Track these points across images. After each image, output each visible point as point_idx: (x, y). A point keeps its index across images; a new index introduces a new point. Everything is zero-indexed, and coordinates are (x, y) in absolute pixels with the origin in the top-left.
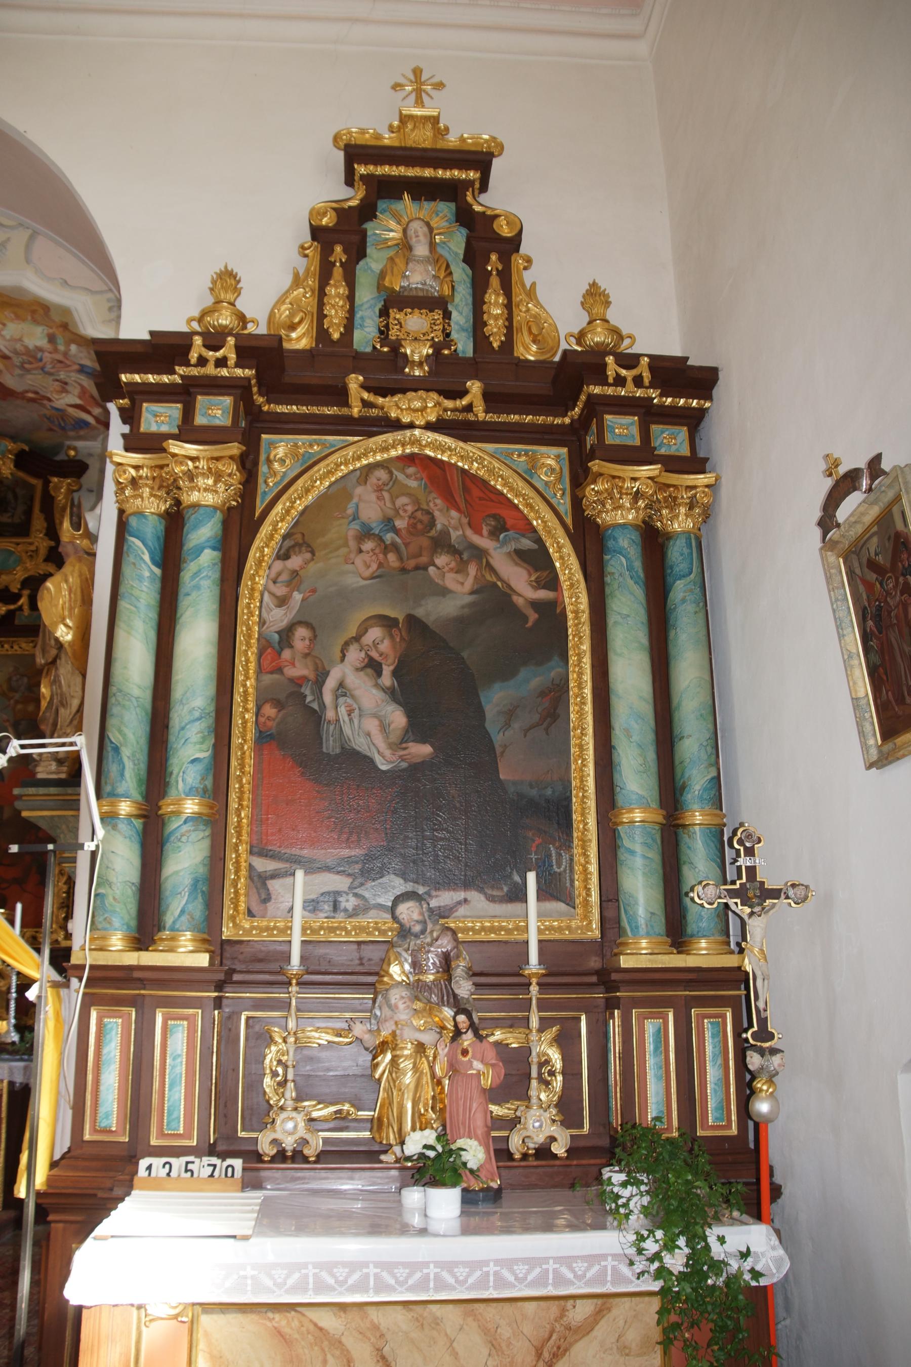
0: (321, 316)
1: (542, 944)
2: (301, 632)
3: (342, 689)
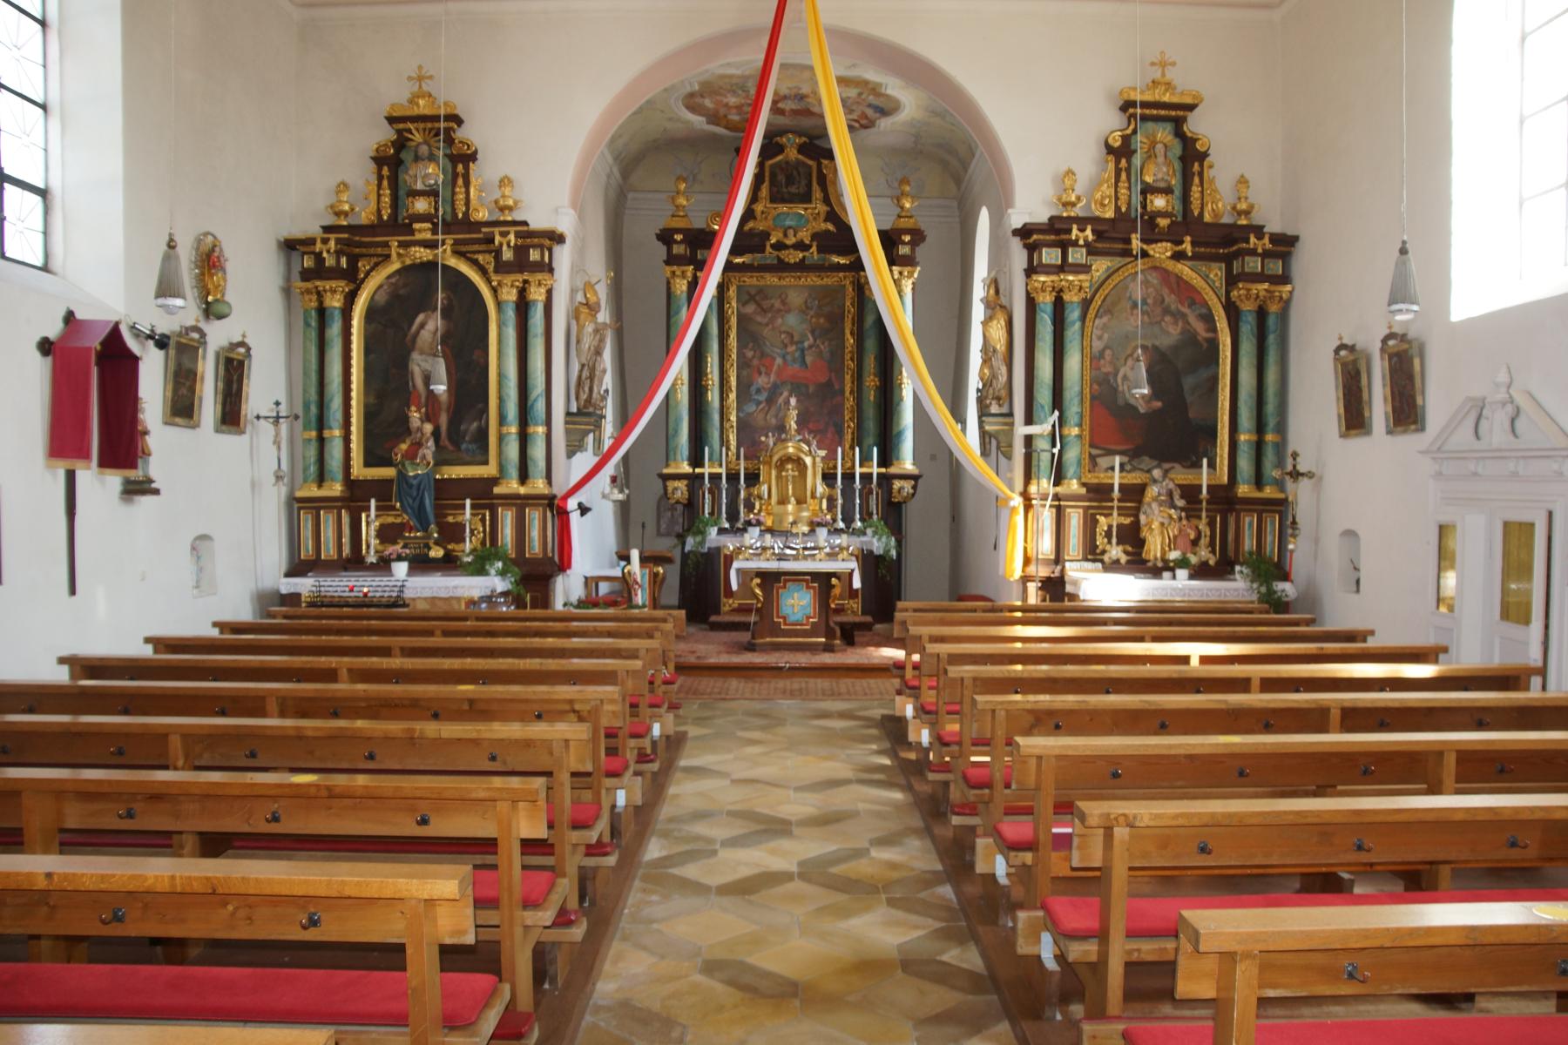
0: (1117, 199)
1: (1209, 486)
2: (1108, 352)
3: (1125, 378)
